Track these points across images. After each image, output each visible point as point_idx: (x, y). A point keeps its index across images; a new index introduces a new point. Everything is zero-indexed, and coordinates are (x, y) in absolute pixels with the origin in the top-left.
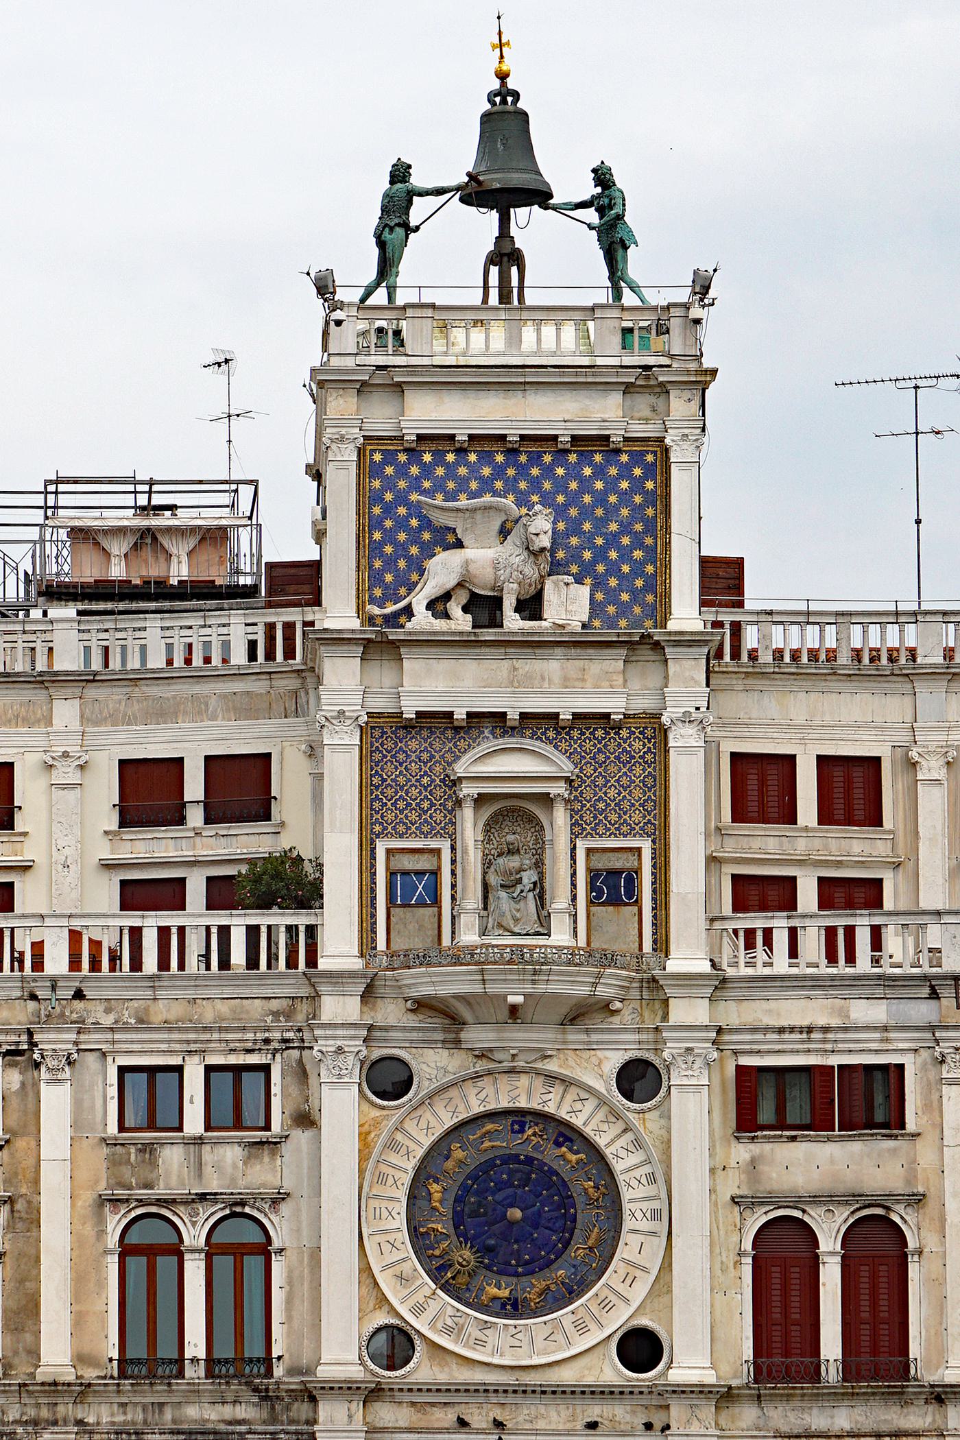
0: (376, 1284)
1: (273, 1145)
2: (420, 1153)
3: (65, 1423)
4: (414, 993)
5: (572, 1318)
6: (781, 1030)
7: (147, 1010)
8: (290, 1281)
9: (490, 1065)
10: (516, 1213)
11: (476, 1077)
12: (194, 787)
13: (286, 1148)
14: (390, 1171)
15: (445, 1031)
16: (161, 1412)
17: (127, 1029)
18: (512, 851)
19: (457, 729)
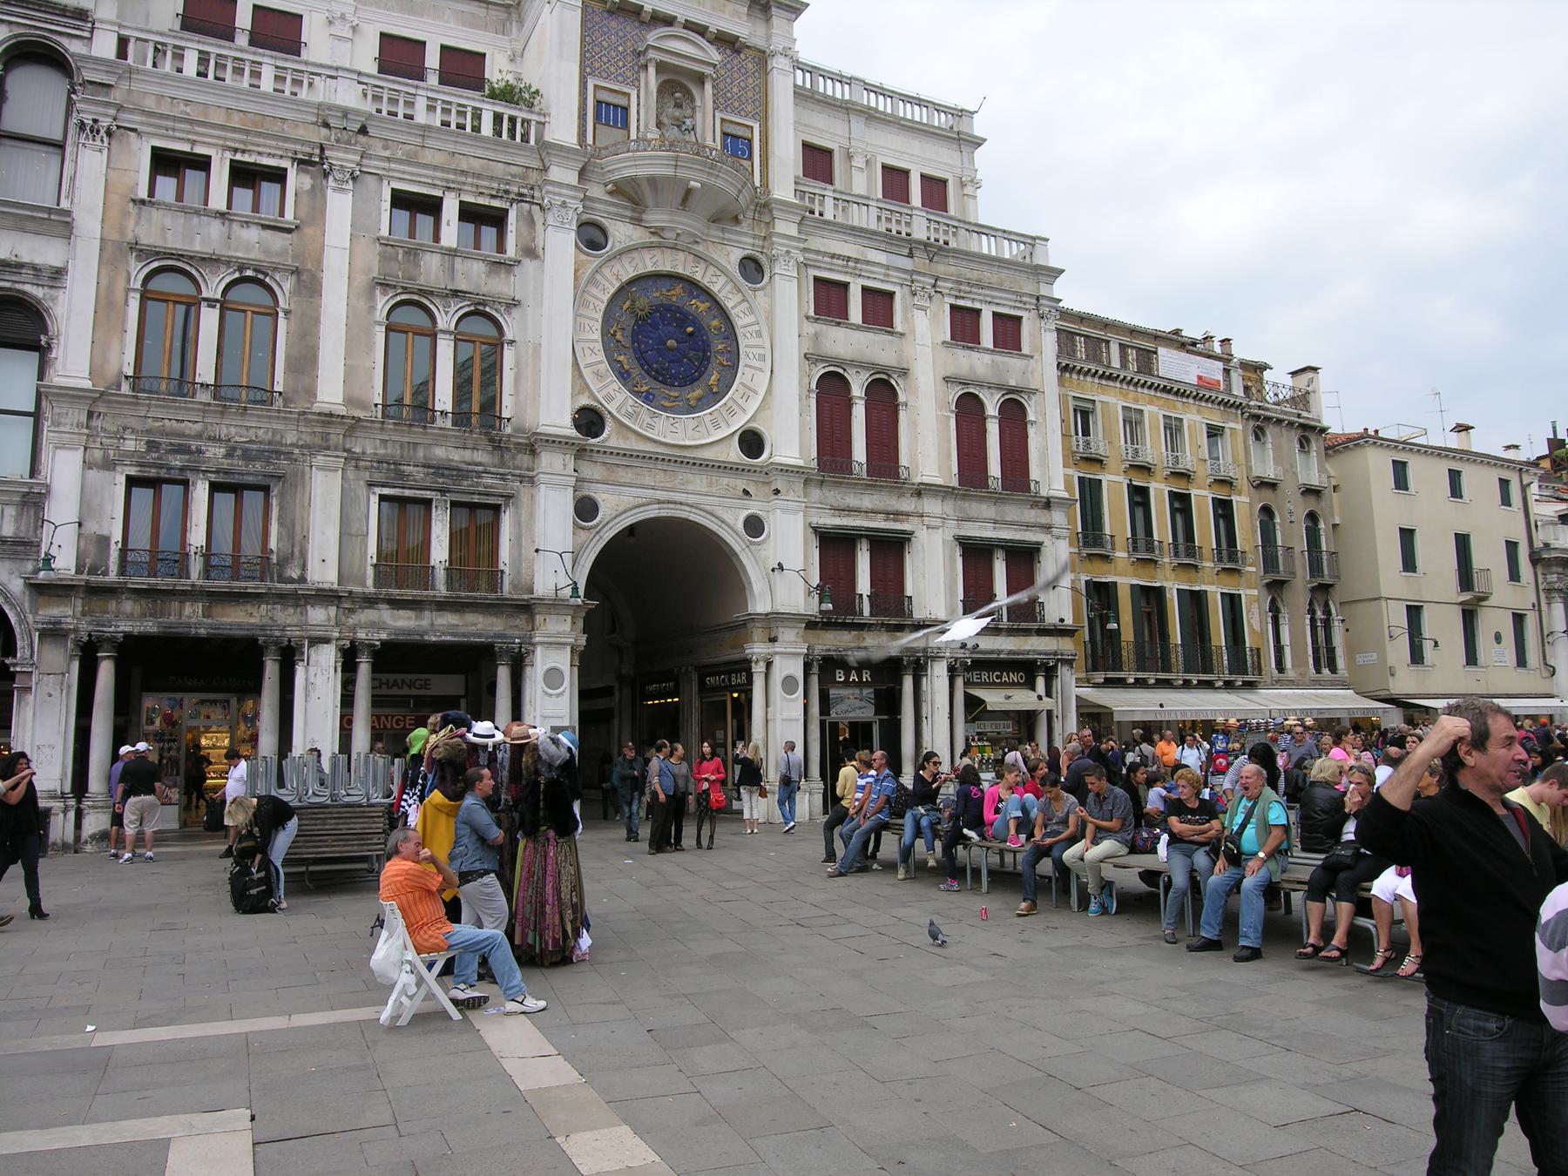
0: (581, 375)
1: (508, 266)
2: (612, 291)
3: (336, 449)
4: (616, 176)
5: (709, 418)
6: (833, 256)
7: (416, 154)
8: (518, 364)
9: (660, 240)
10: (671, 343)
11: (650, 247)
12: (432, 60)
13: (517, 270)
14: (591, 299)
15: (633, 210)
16: (415, 450)
17: (400, 161)
18: (678, 106)
19: (643, 23)
